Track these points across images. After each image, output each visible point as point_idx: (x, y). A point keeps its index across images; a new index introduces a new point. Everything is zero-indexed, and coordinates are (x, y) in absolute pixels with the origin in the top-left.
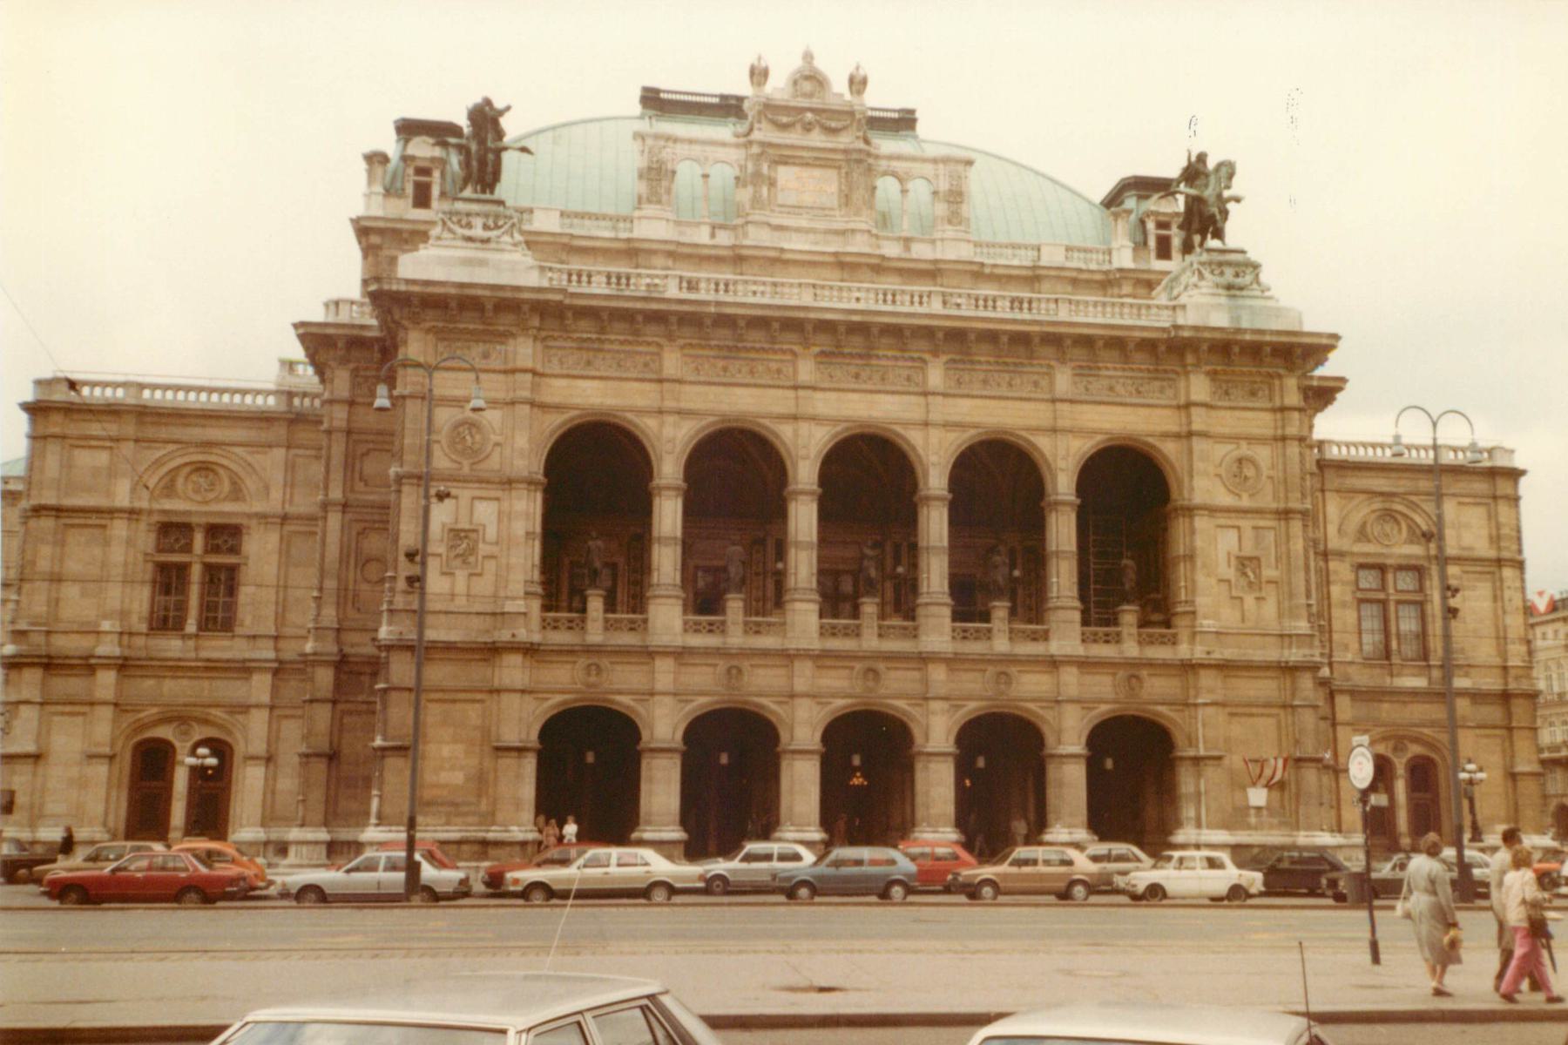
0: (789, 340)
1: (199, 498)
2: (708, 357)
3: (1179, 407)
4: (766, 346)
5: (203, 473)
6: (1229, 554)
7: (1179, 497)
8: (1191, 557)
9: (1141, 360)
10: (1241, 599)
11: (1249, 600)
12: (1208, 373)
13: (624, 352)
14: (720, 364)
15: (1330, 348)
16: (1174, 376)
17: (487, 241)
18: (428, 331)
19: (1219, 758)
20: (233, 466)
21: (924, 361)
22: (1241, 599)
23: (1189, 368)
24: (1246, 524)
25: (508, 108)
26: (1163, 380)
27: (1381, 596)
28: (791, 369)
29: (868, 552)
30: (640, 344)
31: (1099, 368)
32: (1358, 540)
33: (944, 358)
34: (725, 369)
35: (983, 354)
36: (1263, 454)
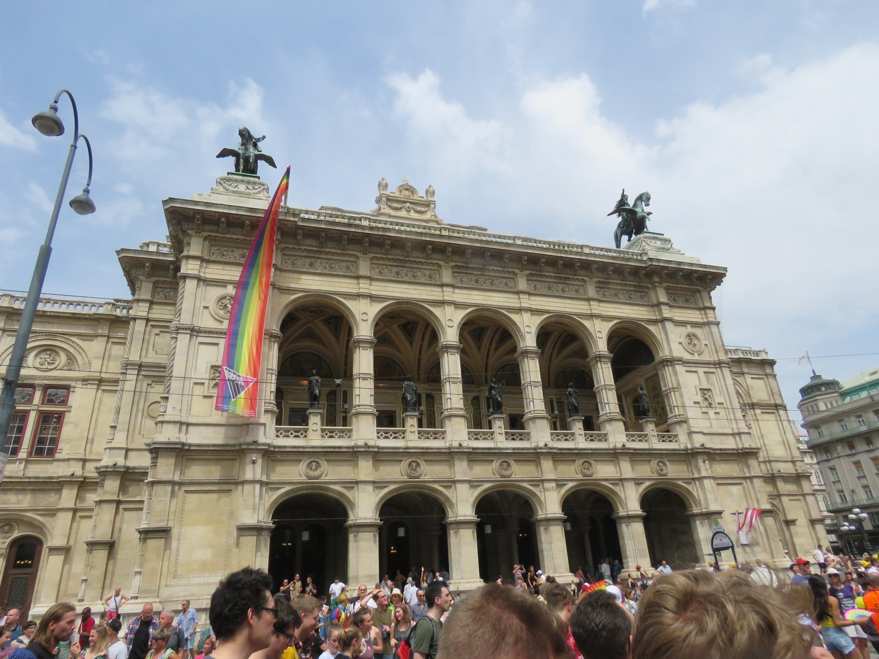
0: (437, 259)
2: (386, 265)
3: (653, 306)
4: (423, 261)
5: (48, 352)
7: (664, 353)
11: (711, 412)
13: (334, 260)
14: (395, 269)
15: (724, 275)
16: (647, 290)
17: (249, 194)
18: (205, 238)
21: (515, 274)
22: (706, 413)
23: (656, 284)
24: (701, 371)
25: (264, 137)
26: (642, 292)
28: (437, 276)
30: (345, 255)
31: (609, 283)
33: (527, 272)
34: (397, 273)
35: (549, 272)
36: (698, 331)
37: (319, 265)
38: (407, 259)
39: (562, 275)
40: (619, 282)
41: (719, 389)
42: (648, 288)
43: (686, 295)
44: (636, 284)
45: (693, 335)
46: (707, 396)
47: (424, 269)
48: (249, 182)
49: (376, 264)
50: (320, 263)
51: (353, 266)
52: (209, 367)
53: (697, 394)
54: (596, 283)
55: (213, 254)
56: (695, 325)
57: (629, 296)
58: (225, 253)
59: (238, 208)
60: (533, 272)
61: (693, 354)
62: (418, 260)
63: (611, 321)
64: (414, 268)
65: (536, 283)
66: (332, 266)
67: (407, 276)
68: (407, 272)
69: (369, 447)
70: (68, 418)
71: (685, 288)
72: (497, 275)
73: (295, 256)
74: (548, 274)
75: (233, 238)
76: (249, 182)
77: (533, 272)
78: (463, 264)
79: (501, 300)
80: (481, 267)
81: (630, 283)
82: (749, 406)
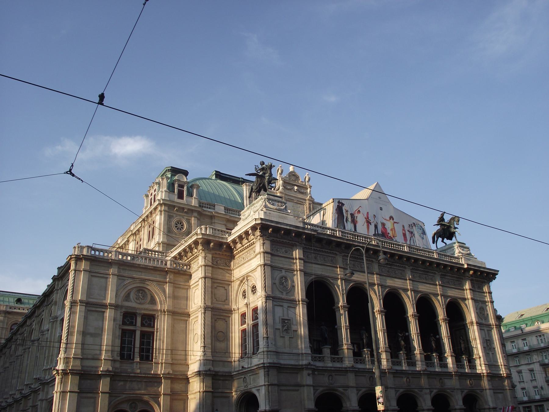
5: (141, 292)
11: (490, 353)
31: (446, 275)
34: (354, 265)
46: (488, 344)
51: (334, 259)
52: (281, 320)
59: (290, 226)
65: (414, 273)
67: (358, 267)
69: (355, 368)
71: (479, 280)
79: (400, 283)
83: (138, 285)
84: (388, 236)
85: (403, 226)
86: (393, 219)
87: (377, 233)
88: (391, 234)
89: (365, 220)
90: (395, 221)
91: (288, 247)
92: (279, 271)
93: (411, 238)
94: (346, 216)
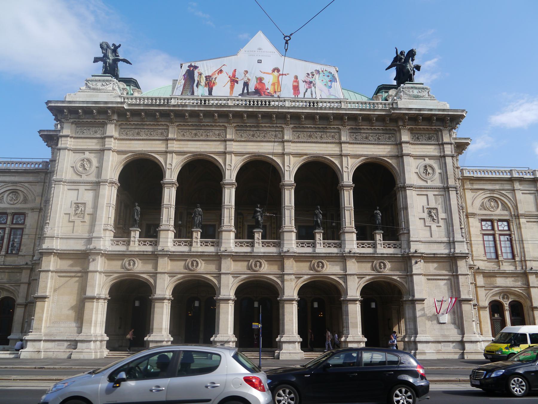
1: (12, 203)
2: (188, 129)
4: (213, 124)
5: (14, 194)
6: (423, 207)
8: (406, 208)
9: (378, 126)
10: (430, 227)
12: (409, 129)
14: (194, 132)
15: (462, 117)
18: (72, 123)
19: (423, 300)
20: (25, 192)
24: (431, 194)
27: (492, 232)
29: (258, 209)
32: (481, 210)
33: (292, 126)
35: (308, 124)
37: (143, 133)
38: (202, 124)
39: (320, 126)
40: (369, 127)
41: (445, 208)
42: (395, 130)
43: (429, 134)
44: (384, 128)
45: (429, 166)
47: (215, 130)
48: (104, 81)
49: (181, 129)
50: (144, 132)
53: (424, 212)
54: (349, 129)
55: (78, 132)
56: (431, 157)
57: (378, 138)
58: (85, 131)
59: (87, 102)
60: (297, 126)
61: (427, 182)
62: (209, 124)
63: (358, 158)
64: (208, 130)
65: (299, 133)
66: (152, 133)
68: (202, 132)
70: (26, 231)
71: (428, 128)
72: (269, 129)
73: (129, 128)
74: (309, 126)
75: (88, 121)
76: (104, 81)
77: (297, 126)
78: (242, 124)
80: (256, 125)
81: (378, 128)
82: (515, 217)
83: (11, 188)
84: (264, 92)
85: (296, 77)
86: (278, 71)
87: (245, 91)
88: (271, 90)
89: (230, 79)
90: (281, 72)
91: (98, 127)
92: (81, 154)
93: (307, 89)
94: (198, 80)
